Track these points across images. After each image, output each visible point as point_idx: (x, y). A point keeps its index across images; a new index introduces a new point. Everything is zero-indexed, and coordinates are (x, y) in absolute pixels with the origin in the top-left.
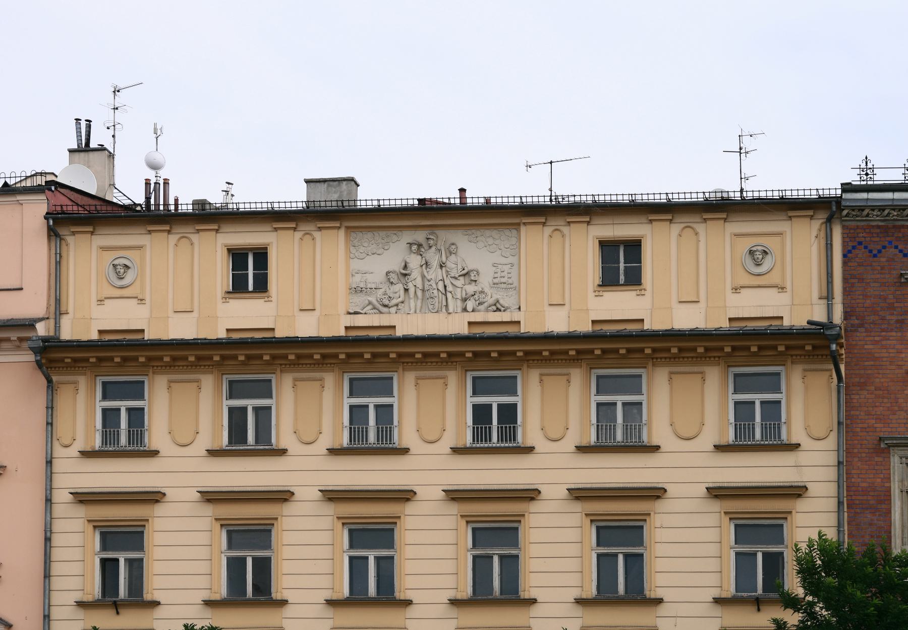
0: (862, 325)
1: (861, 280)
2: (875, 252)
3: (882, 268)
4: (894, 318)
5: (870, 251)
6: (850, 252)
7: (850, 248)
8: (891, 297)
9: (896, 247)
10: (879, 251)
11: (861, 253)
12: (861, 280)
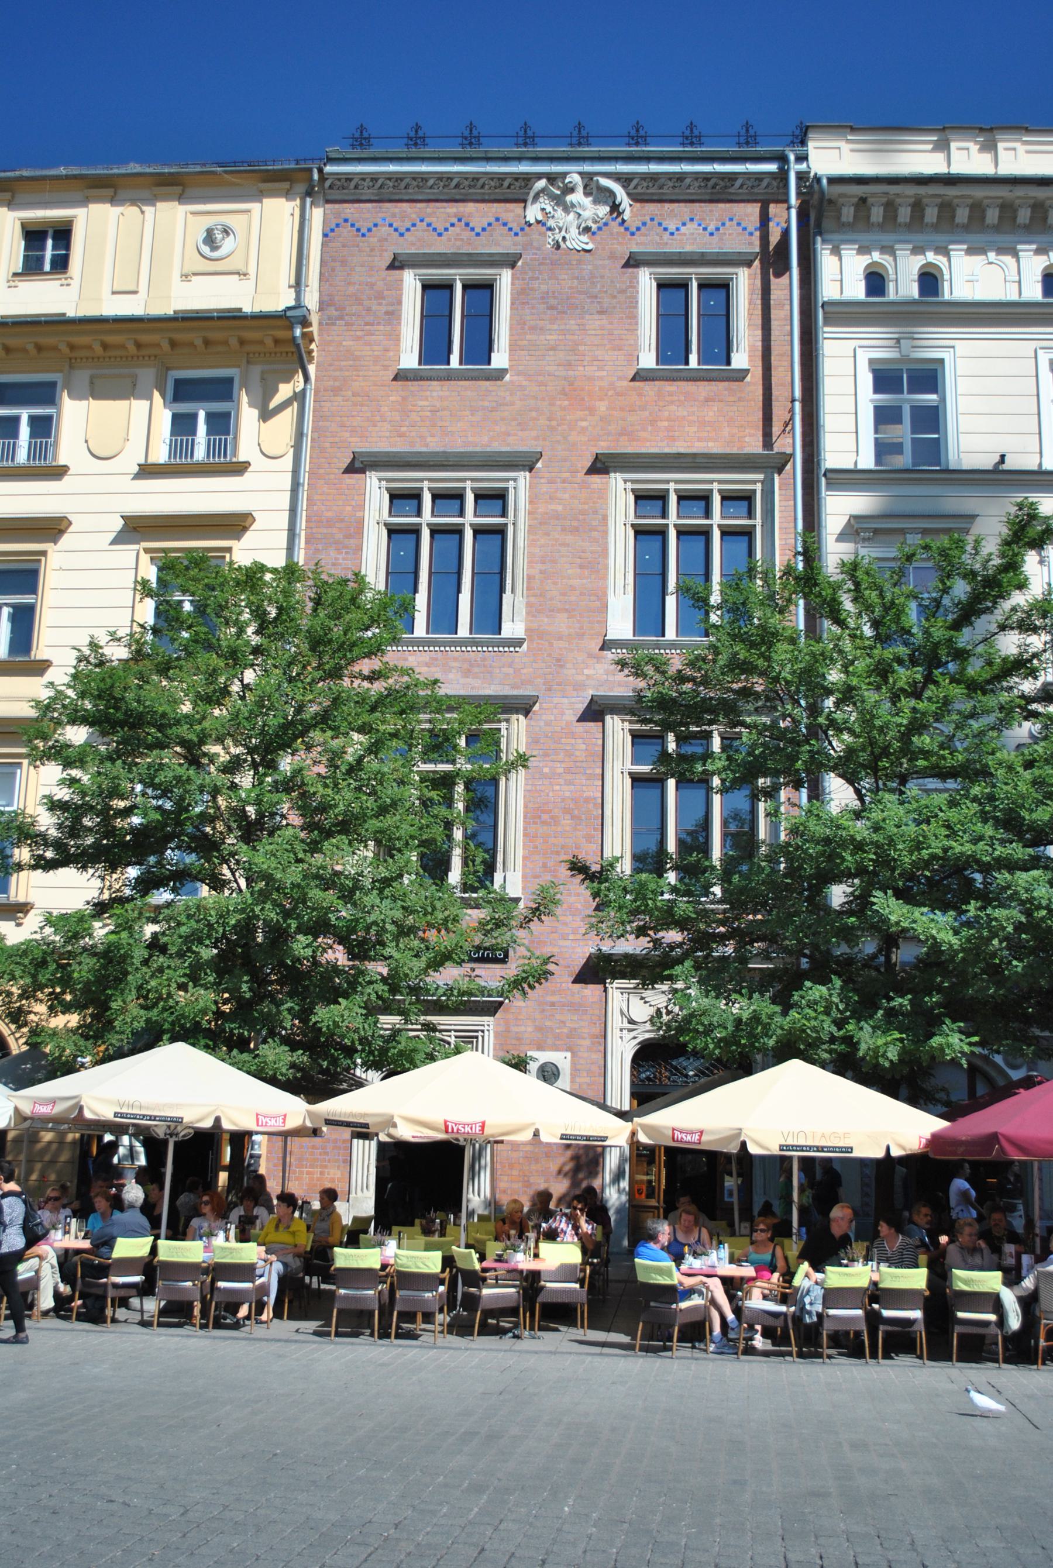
0: (341, 318)
1: (344, 263)
2: (363, 230)
3: (372, 250)
4: (384, 309)
5: (358, 230)
6: (332, 230)
7: (333, 226)
8: (380, 283)
9: (391, 225)
10: (369, 230)
11: (346, 231)
12: (344, 263)
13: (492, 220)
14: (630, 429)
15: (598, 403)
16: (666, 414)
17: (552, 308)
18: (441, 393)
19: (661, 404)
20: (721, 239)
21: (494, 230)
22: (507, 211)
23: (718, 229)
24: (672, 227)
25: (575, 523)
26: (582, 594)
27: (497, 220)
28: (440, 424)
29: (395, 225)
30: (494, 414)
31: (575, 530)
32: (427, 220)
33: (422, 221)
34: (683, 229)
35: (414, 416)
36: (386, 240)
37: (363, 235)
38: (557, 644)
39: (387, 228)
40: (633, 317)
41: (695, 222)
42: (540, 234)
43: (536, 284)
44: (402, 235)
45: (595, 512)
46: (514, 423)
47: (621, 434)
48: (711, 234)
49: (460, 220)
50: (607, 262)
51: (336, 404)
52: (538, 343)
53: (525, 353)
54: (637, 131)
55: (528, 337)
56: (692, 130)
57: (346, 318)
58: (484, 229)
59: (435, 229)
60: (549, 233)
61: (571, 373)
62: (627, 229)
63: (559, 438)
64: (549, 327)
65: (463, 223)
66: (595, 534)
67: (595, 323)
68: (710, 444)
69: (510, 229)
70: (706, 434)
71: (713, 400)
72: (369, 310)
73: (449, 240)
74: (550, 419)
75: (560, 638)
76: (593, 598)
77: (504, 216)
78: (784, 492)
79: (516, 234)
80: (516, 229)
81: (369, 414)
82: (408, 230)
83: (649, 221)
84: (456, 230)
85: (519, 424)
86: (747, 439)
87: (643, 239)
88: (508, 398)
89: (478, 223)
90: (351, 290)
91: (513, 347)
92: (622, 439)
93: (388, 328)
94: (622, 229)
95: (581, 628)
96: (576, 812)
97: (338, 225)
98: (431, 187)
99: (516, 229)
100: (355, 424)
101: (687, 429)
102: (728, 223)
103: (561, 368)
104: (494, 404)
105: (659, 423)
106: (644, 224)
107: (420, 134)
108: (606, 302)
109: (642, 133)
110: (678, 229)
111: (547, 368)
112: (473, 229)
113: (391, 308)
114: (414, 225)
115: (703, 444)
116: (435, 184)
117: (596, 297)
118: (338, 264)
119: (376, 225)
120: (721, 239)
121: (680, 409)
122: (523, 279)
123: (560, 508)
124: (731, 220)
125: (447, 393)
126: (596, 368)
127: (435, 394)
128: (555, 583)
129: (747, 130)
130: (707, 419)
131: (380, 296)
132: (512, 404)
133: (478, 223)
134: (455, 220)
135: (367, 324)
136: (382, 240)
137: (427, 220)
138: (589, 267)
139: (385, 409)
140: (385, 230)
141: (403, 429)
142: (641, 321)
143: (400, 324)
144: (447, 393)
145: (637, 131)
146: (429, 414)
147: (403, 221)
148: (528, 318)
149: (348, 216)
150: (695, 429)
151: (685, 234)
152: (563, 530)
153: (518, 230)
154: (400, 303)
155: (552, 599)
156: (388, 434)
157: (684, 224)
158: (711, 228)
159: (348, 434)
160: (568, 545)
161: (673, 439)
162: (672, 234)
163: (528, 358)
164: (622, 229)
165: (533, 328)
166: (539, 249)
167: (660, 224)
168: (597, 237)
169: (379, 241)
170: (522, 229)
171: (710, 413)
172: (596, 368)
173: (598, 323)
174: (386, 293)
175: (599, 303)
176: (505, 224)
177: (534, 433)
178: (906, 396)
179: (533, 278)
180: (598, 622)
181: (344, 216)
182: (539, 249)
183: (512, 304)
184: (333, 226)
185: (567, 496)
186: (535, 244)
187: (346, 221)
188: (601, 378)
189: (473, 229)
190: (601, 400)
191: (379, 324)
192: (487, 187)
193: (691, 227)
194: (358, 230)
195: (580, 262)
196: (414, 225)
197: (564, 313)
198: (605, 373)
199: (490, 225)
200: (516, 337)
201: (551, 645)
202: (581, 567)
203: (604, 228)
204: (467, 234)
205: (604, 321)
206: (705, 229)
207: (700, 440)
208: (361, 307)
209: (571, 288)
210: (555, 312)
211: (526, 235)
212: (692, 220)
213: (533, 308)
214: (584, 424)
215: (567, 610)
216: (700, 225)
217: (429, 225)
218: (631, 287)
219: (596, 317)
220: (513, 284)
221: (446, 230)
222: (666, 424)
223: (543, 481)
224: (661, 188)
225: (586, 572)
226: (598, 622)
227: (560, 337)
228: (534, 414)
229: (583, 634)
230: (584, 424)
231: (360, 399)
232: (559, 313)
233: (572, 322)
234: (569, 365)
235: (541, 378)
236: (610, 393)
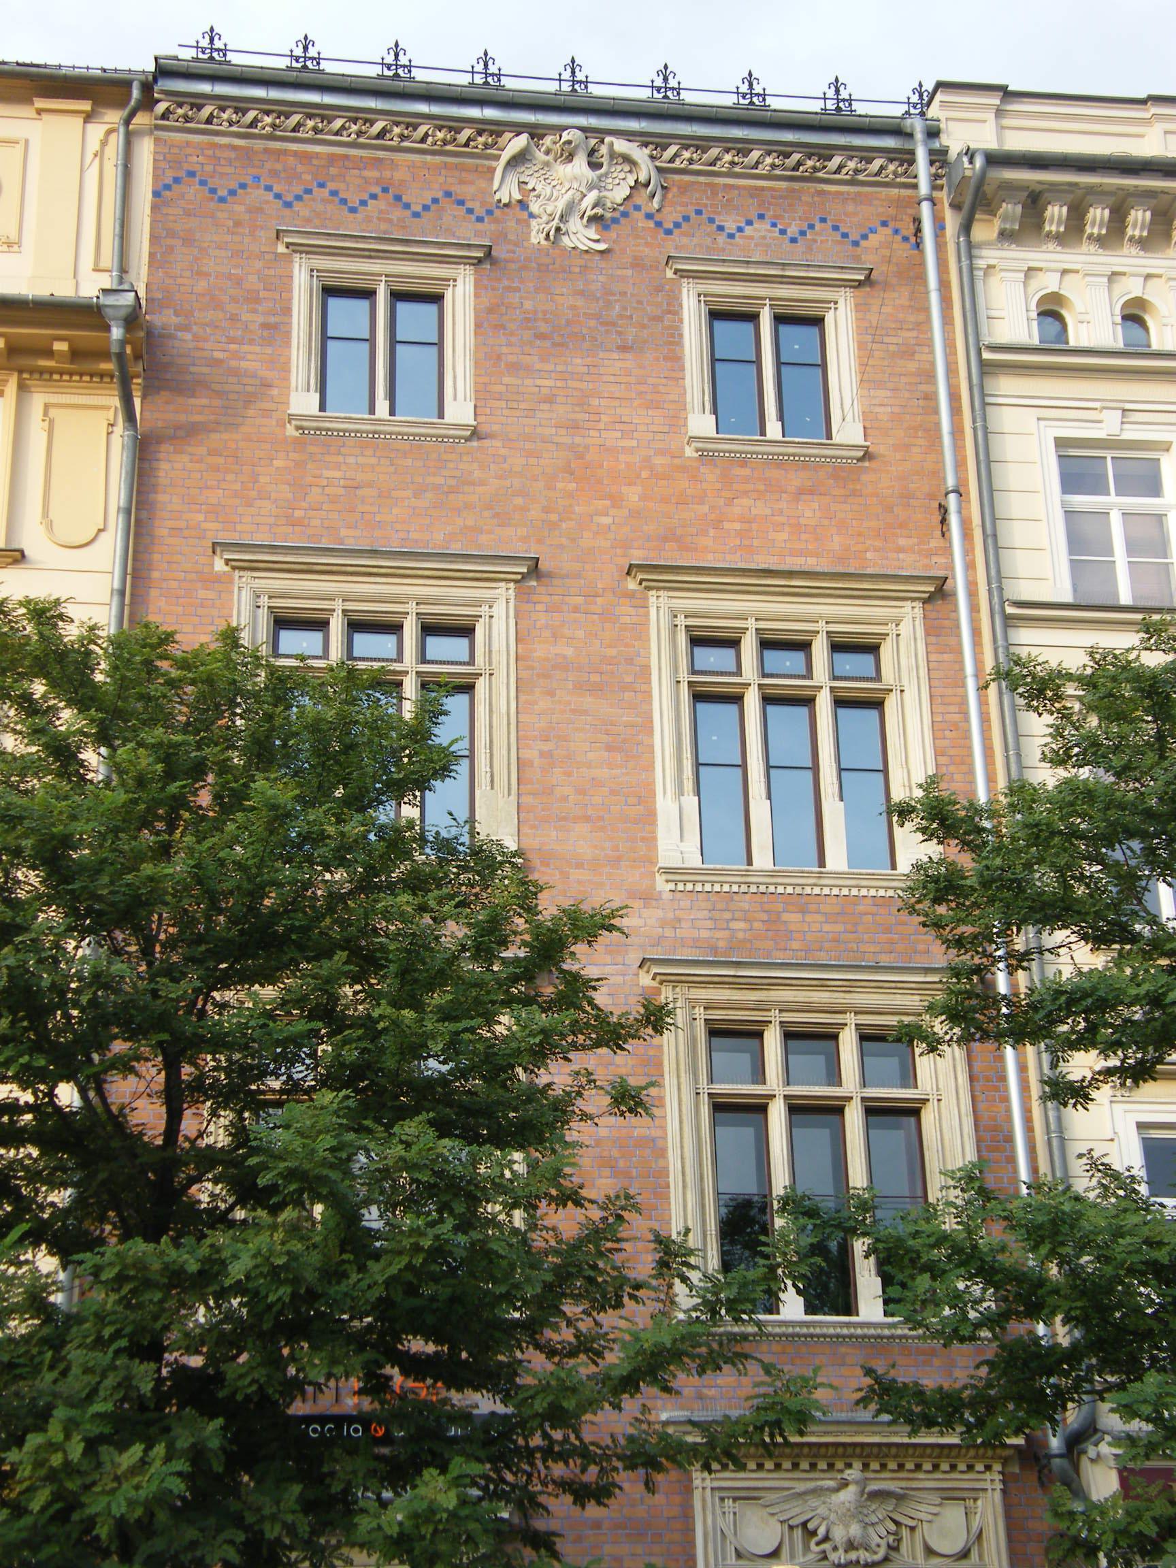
1: (188, 241)
2: (222, 192)
3: (238, 224)
4: (261, 319)
6: (168, 187)
7: (169, 181)
8: (253, 278)
9: (269, 188)
11: (192, 191)
12: (188, 241)
13: (440, 195)
14: (679, 532)
15: (624, 489)
16: (737, 510)
17: (541, 336)
18: (361, 460)
19: (726, 494)
20: (810, 249)
21: (443, 209)
22: (461, 182)
23: (803, 233)
24: (731, 226)
25: (595, 678)
26: (613, 792)
27: (448, 194)
28: (360, 508)
29: (276, 189)
30: (451, 496)
31: (596, 689)
32: (331, 186)
33: (322, 185)
34: (748, 230)
35: (315, 494)
36: (260, 210)
37: (222, 200)
38: (575, 874)
39: (262, 192)
40: (675, 358)
41: (768, 221)
42: (518, 221)
43: (514, 298)
44: (288, 205)
45: (630, 661)
46: (487, 514)
47: (665, 539)
48: (794, 240)
49: (385, 190)
50: (629, 272)
51: (177, 466)
52: (521, 389)
53: (503, 404)
54: (666, 79)
55: (506, 380)
56: (751, 85)
57: (195, 328)
58: (426, 208)
59: (344, 201)
60: (534, 223)
61: (578, 440)
62: (659, 224)
63: (564, 541)
64: (538, 366)
65: (390, 195)
66: (628, 695)
67: (614, 364)
69: (470, 211)
70: (803, 546)
71: (811, 493)
72: (234, 318)
73: (369, 219)
74: (546, 510)
75: (579, 865)
76: (631, 800)
77: (459, 190)
78: (933, 639)
79: (480, 219)
80: (480, 211)
81: (238, 487)
82: (298, 198)
83: (693, 215)
84: (381, 204)
85: (497, 515)
86: (869, 555)
87: (685, 240)
88: (477, 474)
89: (417, 196)
90: (202, 285)
91: (482, 396)
92: (667, 545)
93: (269, 351)
94: (651, 224)
95: (616, 849)
96: (621, 1164)
97: (177, 180)
98: (337, 133)
99: (480, 211)
100: (213, 501)
101: (772, 535)
102: (818, 226)
103: (563, 431)
104: (452, 482)
105: (727, 525)
106: (686, 219)
107: (312, 52)
108: (631, 333)
109: (672, 83)
110: (740, 230)
111: (539, 430)
112: (407, 206)
113: (273, 320)
114: (308, 191)
115: (801, 561)
116: (343, 127)
117: (614, 324)
118: (177, 242)
119: (243, 186)
120: (810, 249)
121: (759, 503)
122: (493, 289)
123: (569, 652)
124: (823, 220)
125: (373, 461)
126: (619, 435)
127: (351, 460)
128: (569, 774)
129: (837, 91)
130: (802, 521)
131: (253, 299)
132: (482, 483)
133: (417, 196)
134: (377, 190)
135: (232, 341)
136: (256, 210)
137: (331, 186)
138: (601, 278)
139: (263, 479)
140: (257, 195)
141: (298, 513)
142: (687, 365)
143: (288, 344)
144: (373, 461)
145: (666, 79)
146: (342, 491)
147: (290, 184)
148: (504, 350)
149: (198, 168)
151: (751, 238)
152: (579, 687)
153: (483, 214)
154: (287, 311)
155: (565, 799)
156: (272, 520)
157: (749, 223)
158: (793, 230)
159: (201, 517)
160: (586, 713)
162: (731, 236)
163: (506, 412)
164: (651, 224)
165: (514, 368)
166: (516, 245)
167: (711, 220)
168: (613, 234)
169: (249, 211)
170: (489, 212)
171: (809, 511)
172: (619, 435)
173: (619, 364)
174: (262, 294)
175: (619, 333)
176: (461, 203)
177: (522, 532)
178: (1113, 498)
179: (509, 289)
180: (643, 839)
181: (186, 166)
182: (516, 245)
183: (478, 325)
184: (169, 181)
185: (580, 634)
186: (511, 237)
187: (192, 174)
188: (629, 451)
189: (407, 206)
191: (252, 342)
192: (430, 139)
193: (762, 228)
194: (213, 191)
195: (585, 269)
196: (308, 191)
197: (561, 345)
198: (634, 443)
199: (435, 201)
200: (486, 380)
201: (565, 875)
202: (609, 748)
203: (623, 220)
204: (397, 214)
205: (629, 361)
206: (783, 232)
207: (793, 553)
208: (220, 315)
209: (573, 308)
210: (548, 344)
211: (497, 221)
212: (761, 217)
213: (512, 334)
214: (607, 520)
215: (587, 819)
216: (774, 225)
217: (334, 193)
218: (670, 312)
219: (615, 356)
220: (477, 296)
221: (363, 203)
222: (737, 526)
223: (539, 607)
224: (713, 164)
225: (618, 757)
226: (643, 839)
227: (559, 384)
228: (519, 501)
229: (619, 859)
230: (607, 520)
231: (221, 460)
232: (554, 345)
233: (579, 361)
234: (574, 427)
235: (528, 445)
236: (644, 474)
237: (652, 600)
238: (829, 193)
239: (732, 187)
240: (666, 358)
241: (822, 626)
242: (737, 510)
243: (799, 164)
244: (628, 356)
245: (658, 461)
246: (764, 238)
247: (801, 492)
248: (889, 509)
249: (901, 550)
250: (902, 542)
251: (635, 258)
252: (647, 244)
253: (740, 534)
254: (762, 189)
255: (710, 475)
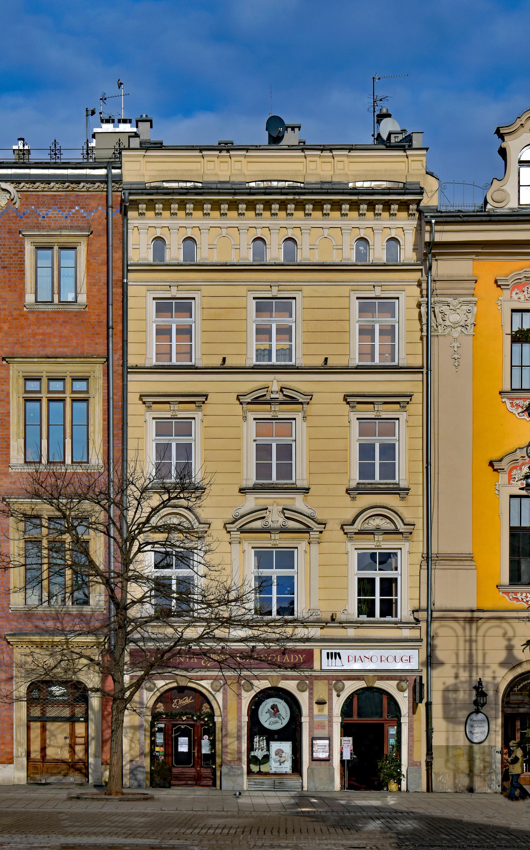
40: (22, 271)
47: (16, 343)
68: (66, 350)
120: (72, 220)
130: (63, 334)
150: (57, 340)
151: (51, 217)
161: (44, 346)
171: (66, 331)
188: (4, 309)
190: (5, 322)
207: (60, 347)
218: (21, 251)
222: (41, 337)
224: (37, 188)
237: (11, 368)
238: (80, 195)
239: (44, 195)
240: (19, 271)
241: (68, 374)
242: (41, 331)
243: (68, 186)
244: (6, 269)
245: (15, 313)
246: (55, 217)
247: (64, 322)
248: (94, 328)
249: (97, 344)
250: (97, 341)
251: (9, 229)
252: (14, 223)
253: (41, 340)
254: (55, 196)
255: (32, 317)
